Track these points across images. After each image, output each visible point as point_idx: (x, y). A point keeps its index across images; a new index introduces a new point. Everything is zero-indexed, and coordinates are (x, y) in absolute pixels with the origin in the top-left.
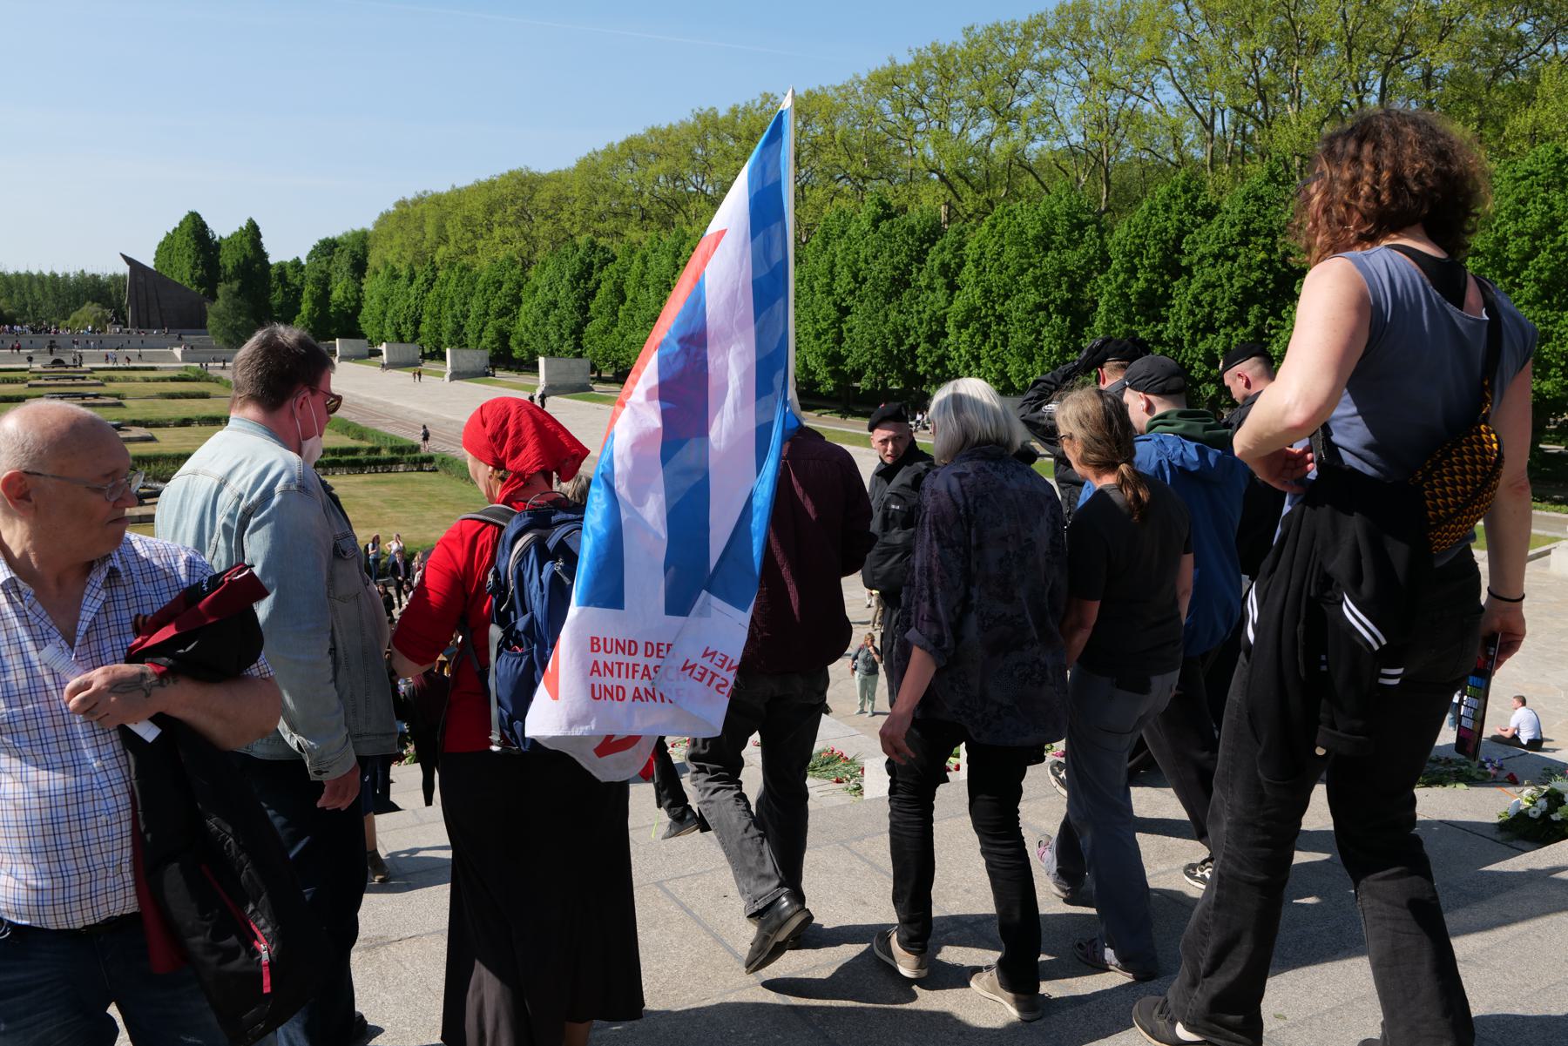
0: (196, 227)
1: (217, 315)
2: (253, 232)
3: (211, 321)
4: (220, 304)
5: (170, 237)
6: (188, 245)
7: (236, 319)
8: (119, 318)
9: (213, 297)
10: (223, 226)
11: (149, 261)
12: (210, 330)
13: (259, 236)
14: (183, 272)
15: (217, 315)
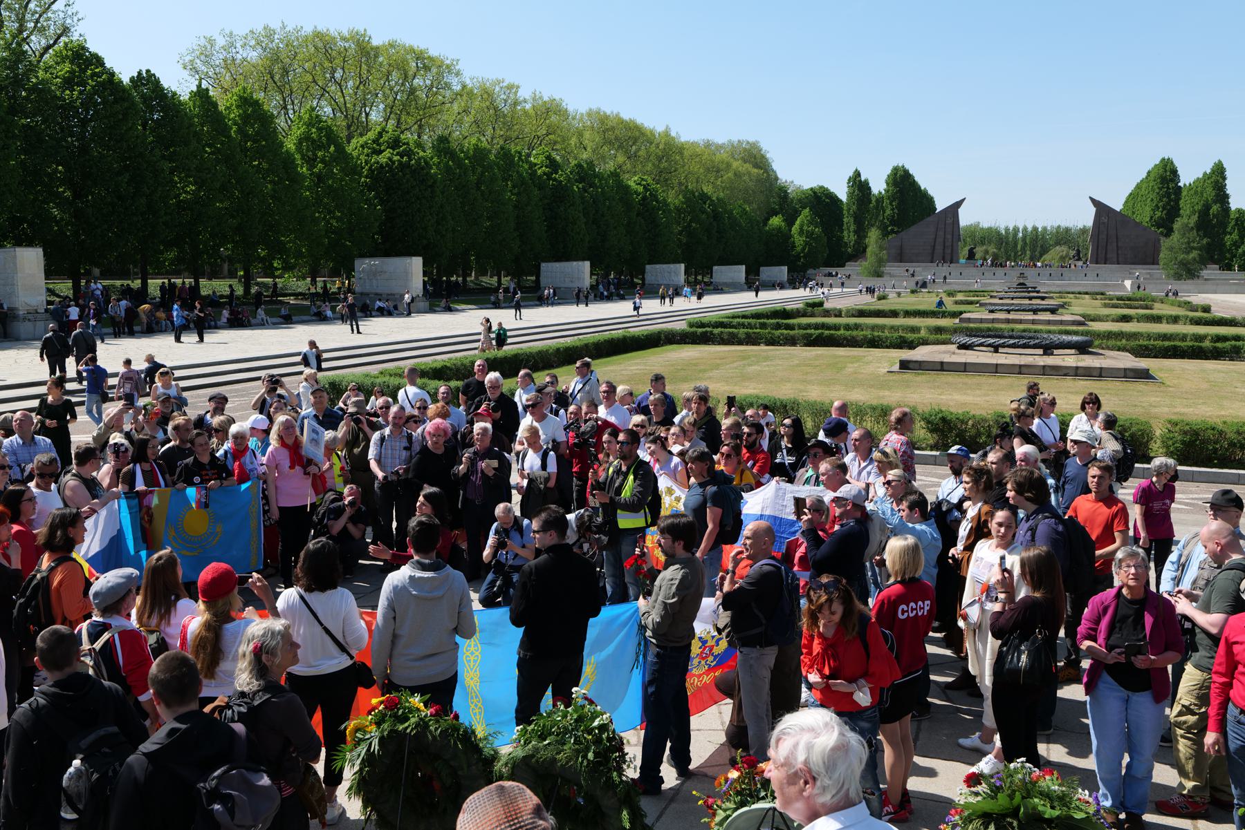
0: (1166, 175)
1: (1171, 249)
2: (1218, 175)
3: (1163, 255)
4: (1175, 236)
5: (1138, 187)
6: (1153, 190)
7: (1188, 253)
8: (1078, 257)
9: (1169, 232)
10: (1187, 177)
11: (1117, 204)
12: (1161, 263)
13: (1224, 179)
14: (1144, 215)
15: (1171, 249)
